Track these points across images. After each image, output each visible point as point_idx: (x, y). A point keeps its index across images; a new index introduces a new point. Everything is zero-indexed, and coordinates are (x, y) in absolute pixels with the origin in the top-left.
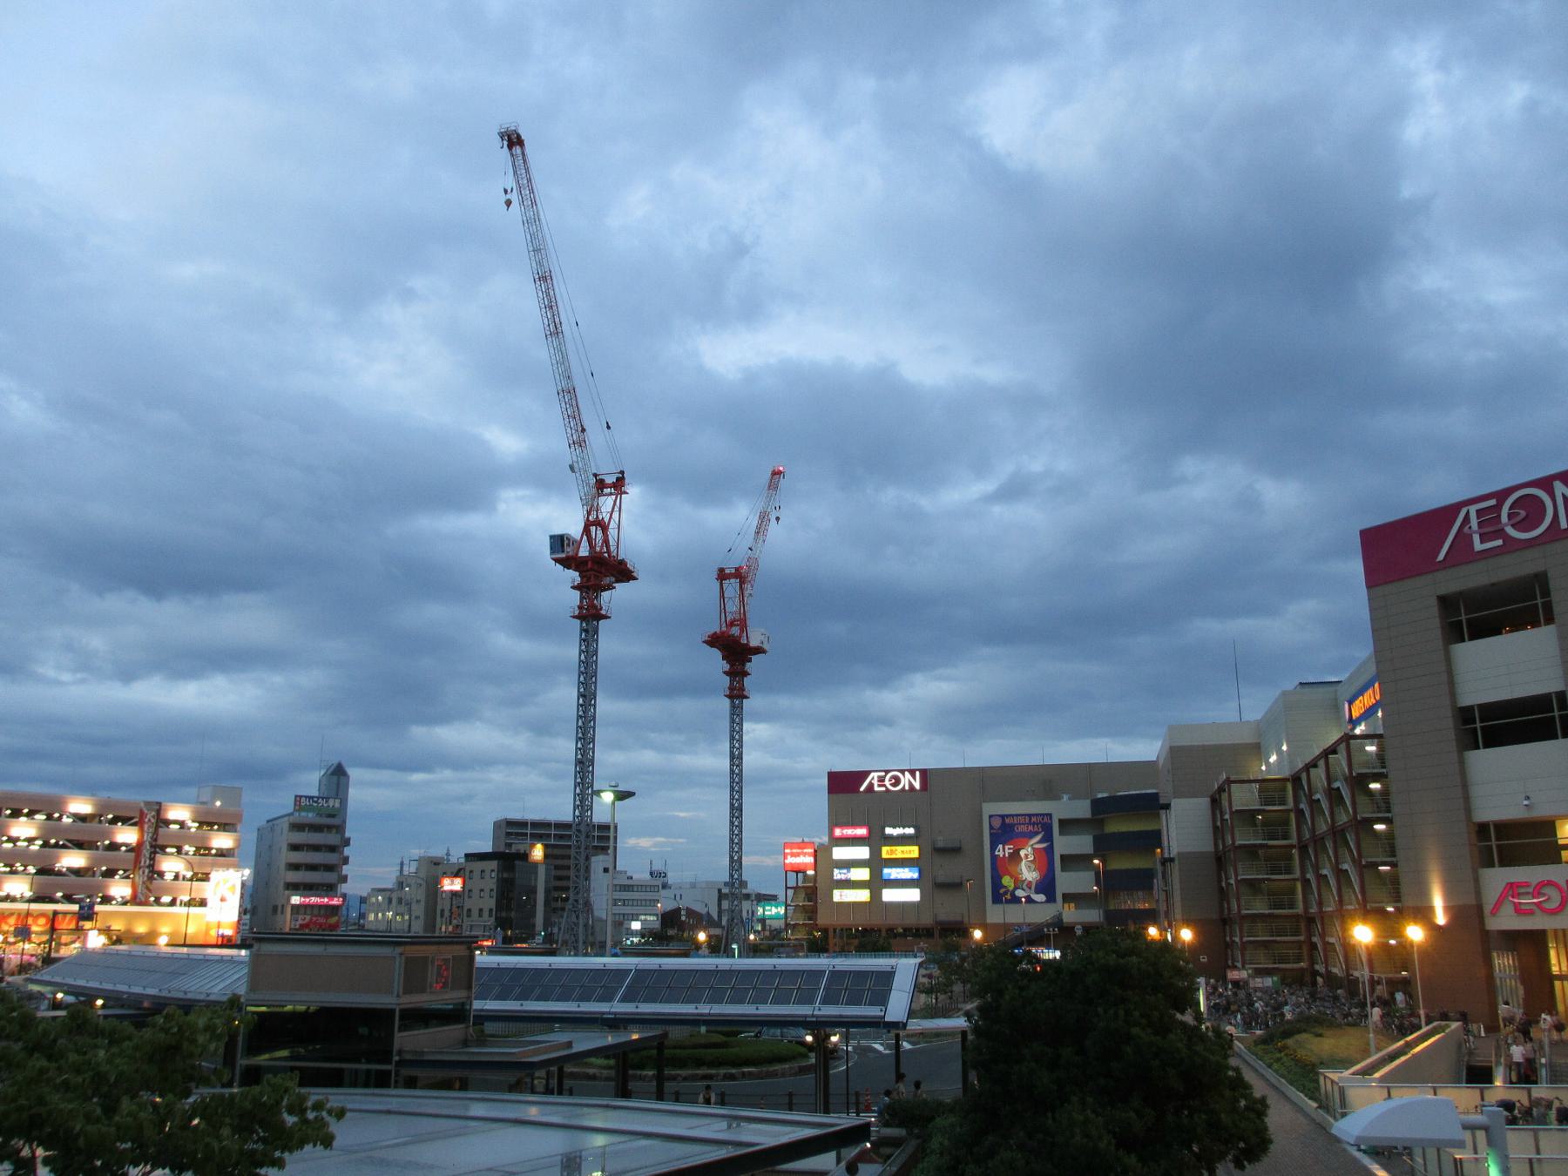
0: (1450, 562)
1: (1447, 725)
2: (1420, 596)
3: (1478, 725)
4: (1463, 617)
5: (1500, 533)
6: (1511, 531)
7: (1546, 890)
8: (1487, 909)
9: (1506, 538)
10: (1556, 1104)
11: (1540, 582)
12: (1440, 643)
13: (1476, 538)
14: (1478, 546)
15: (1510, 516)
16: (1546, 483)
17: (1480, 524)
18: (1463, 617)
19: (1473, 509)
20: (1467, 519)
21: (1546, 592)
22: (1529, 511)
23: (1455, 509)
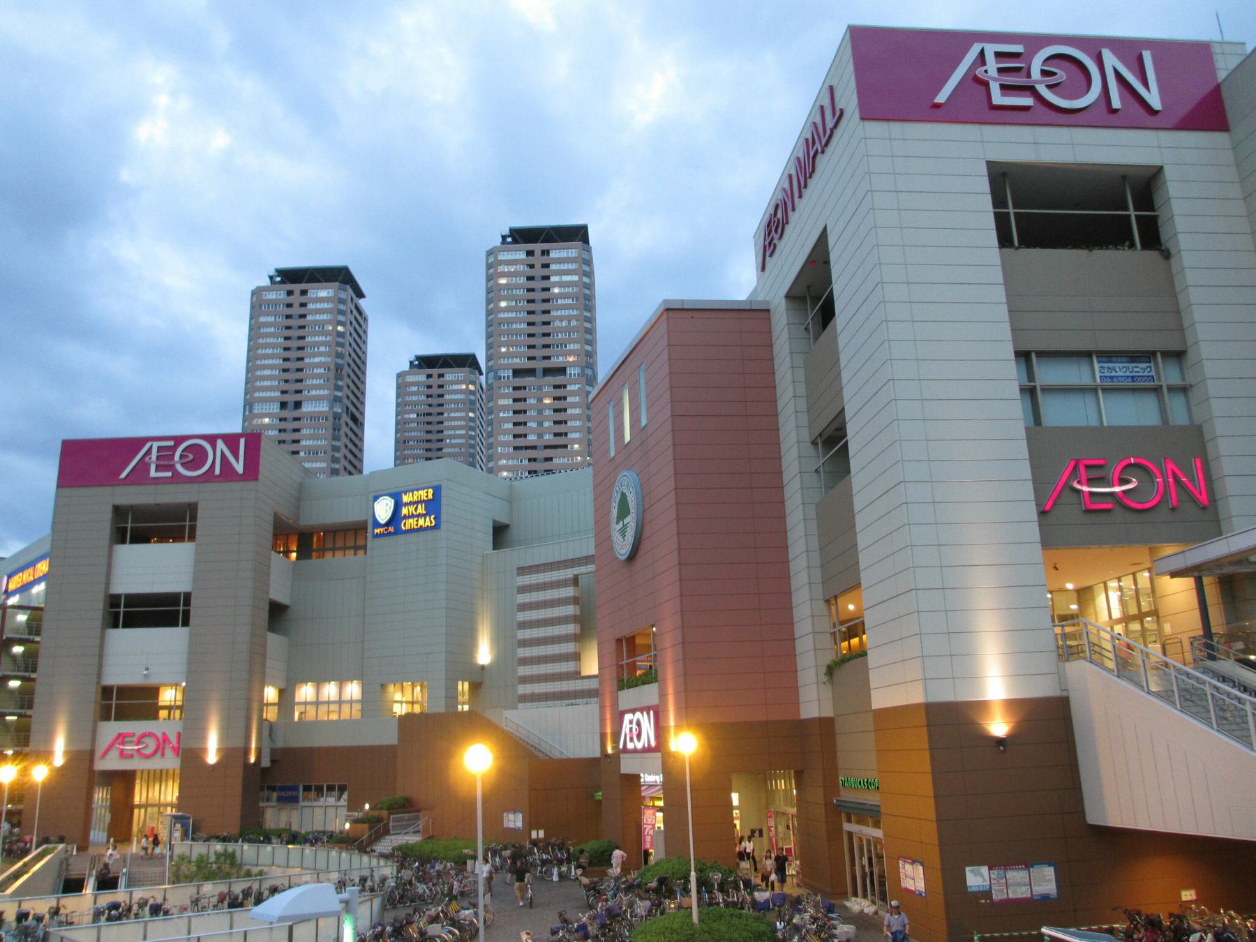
0: (129, 481)
1: (97, 609)
2: (99, 503)
3: (122, 609)
4: (129, 525)
5: (171, 467)
6: (179, 468)
7: (147, 740)
8: (98, 754)
9: (176, 474)
10: (151, 902)
11: (192, 509)
12: (107, 542)
13: (153, 467)
14: (153, 473)
15: (182, 457)
16: (212, 439)
17: (158, 458)
18: (129, 525)
19: (156, 445)
20: (149, 452)
21: (194, 518)
22: (196, 456)
23: (141, 442)
